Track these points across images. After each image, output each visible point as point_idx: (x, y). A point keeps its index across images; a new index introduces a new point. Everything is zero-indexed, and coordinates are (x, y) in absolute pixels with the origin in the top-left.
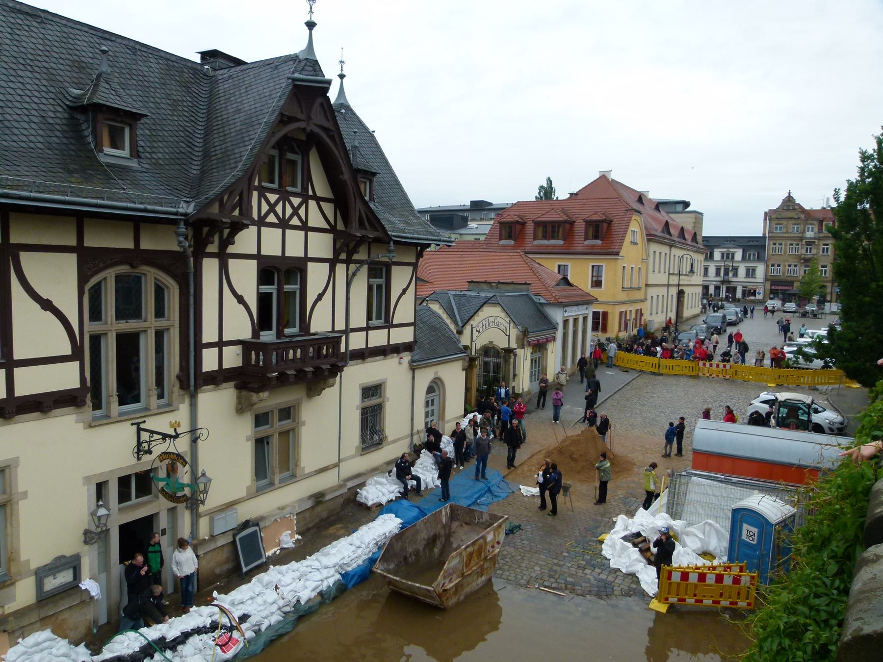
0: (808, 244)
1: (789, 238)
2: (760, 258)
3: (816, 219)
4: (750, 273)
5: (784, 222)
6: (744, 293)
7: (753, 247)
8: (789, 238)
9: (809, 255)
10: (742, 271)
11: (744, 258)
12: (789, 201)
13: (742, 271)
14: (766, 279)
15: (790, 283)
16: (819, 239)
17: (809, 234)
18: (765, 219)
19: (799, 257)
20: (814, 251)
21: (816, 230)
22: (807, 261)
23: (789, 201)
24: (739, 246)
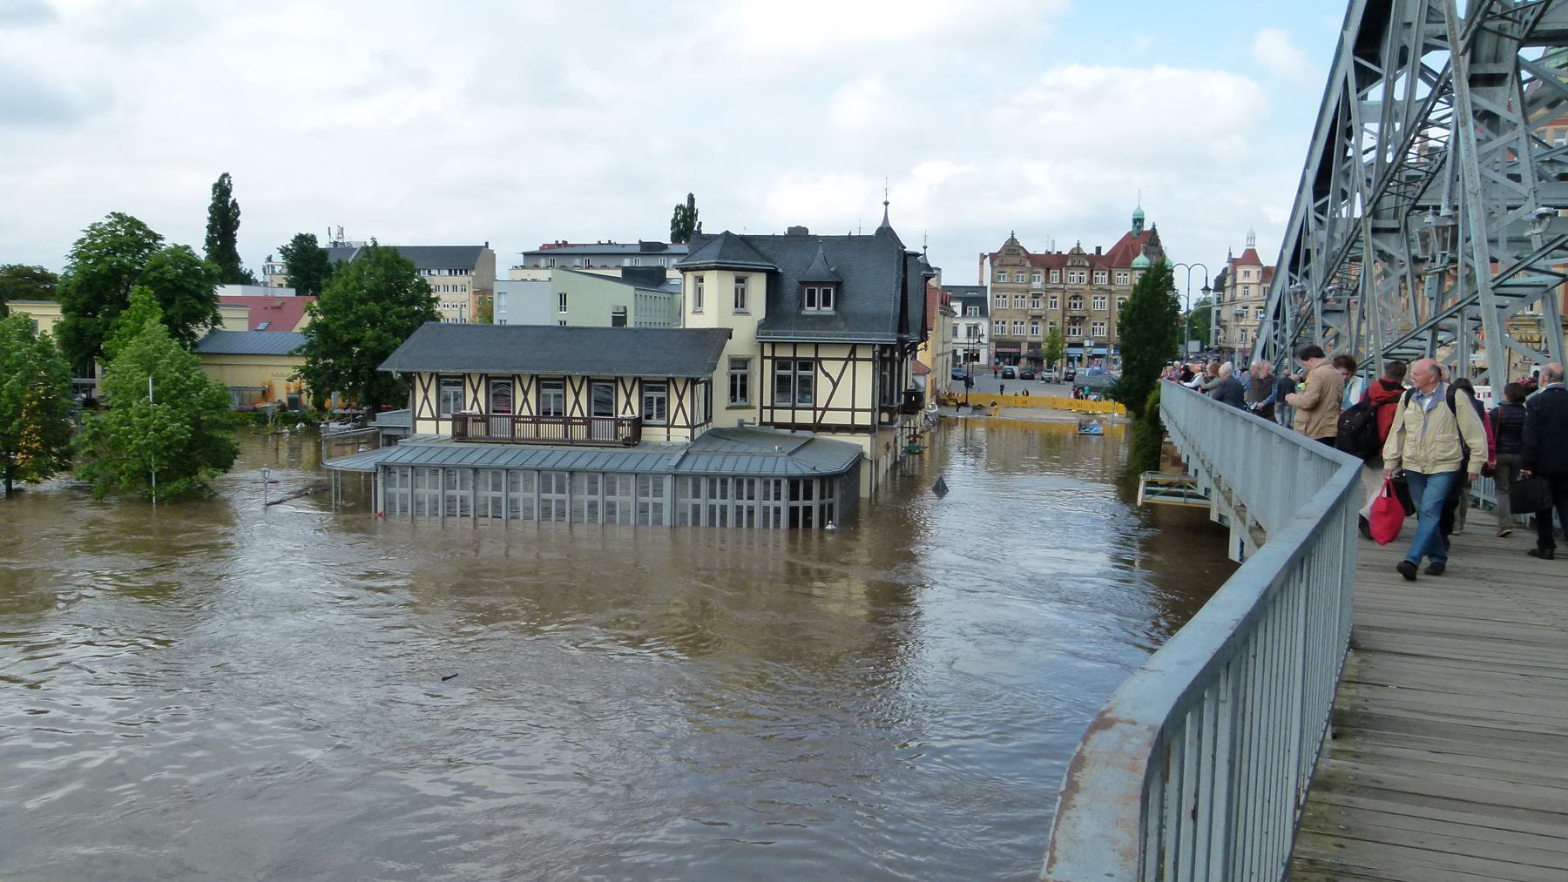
0: (1035, 296)
1: (1013, 290)
2: (984, 313)
3: (1042, 266)
4: (972, 331)
5: (1008, 270)
6: (966, 356)
7: (973, 299)
8: (1013, 290)
9: (1036, 311)
10: (962, 331)
11: (964, 311)
12: (1013, 240)
13: (962, 331)
14: (991, 340)
15: (1017, 345)
16: (1047, 291)
17: (1037, 285)
18: (982, 263)
19: (1026, 312)
20: (1042, 305)
21: (1043, 279)
22: (1036, 318)
23: (1013, 240)
24: (957, 299)
